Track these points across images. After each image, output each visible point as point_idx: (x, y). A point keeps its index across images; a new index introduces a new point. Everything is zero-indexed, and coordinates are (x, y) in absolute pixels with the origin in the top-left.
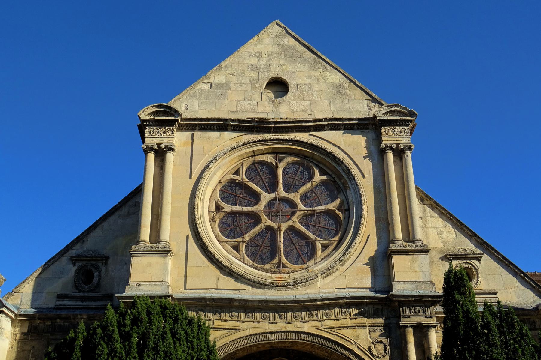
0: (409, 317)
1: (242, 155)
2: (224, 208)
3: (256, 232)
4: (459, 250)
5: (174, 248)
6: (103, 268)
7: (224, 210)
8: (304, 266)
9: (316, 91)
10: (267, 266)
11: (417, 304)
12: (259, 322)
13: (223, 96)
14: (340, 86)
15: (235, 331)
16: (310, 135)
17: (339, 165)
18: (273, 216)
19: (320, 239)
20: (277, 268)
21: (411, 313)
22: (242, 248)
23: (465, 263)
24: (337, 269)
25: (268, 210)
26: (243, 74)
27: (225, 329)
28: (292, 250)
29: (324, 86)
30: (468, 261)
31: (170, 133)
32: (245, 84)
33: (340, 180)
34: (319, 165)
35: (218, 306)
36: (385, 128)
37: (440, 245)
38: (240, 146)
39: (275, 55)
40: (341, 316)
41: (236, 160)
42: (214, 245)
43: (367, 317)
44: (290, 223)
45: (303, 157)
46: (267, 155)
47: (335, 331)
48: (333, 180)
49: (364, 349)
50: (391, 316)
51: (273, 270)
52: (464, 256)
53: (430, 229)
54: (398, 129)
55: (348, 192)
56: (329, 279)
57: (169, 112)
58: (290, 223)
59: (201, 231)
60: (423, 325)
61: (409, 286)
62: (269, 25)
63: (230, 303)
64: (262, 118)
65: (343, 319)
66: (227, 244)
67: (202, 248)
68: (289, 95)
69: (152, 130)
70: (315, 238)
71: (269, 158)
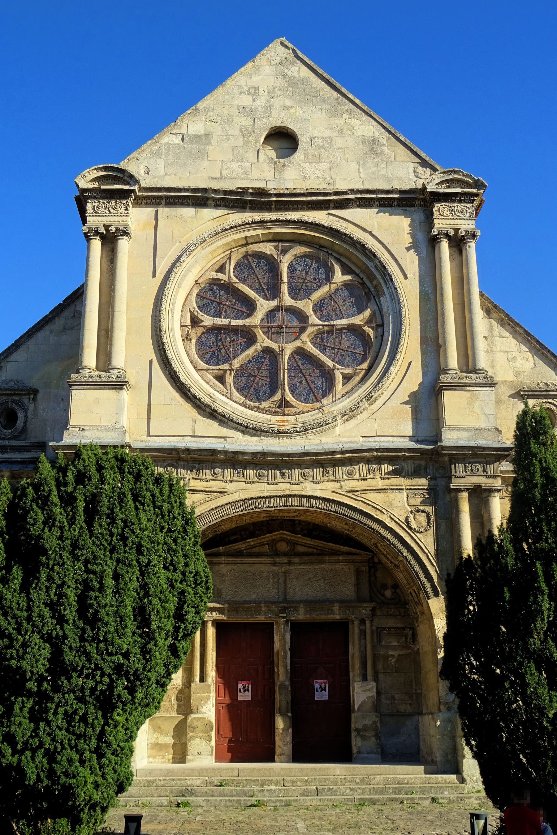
0: (463, 477)
1: (228, 244)
2: (202, 321)
3: (248, 356)
4: (538, 384)
5: (131, 377)
6: (31, 405)
7: (202, 324)
8: (318, 405)
9: (339, 148)
10: (265, 405)
11: (476, 460)
12: (253, 483)
13: (201, 154)
14: (374, 141)
15: (219, 494)
16: (329, 214)
17: (370, 259)
18: (274, 333)
19: (340, 367)
20: (279, 407)
21: (466, 471)
22: (229, 378)
23: (546, 402)
24: (364, 410)
25: (266, 324)
26: (230, 121)
28: (301, 382)
29: (350, 141)
30: (550, 401)
31: (123, 210)
32: (234, 137)
33: (371, 282)
34: (341, 259)
35: (195, 460)
36: (439, 205)
37: (510, 377)
38: (226, 230)
39: (279, 92)
40: (368, 475)
41: (221, 251)
42: (188, 374)
43: (404, 477)
44: (298, 343)
45: (318, 247)
46: (265, 244)
47: (360, 496)
48: (361, 281)
49: (400, 520)
50: (438, 475)
51: (273, 410)
52: (545, 393)
53: (498, 354)
54: (458, 206)
55: (382, 299)
56: (353, 422)
57: (122, 178)
58: (298, 343)
59: (170, 353)
60: (483, 488)
61: (465, 434)
62: (270, 45)
63: (212, 455)
64: (258, 189)
65: (371, 478)
66: (208, 373)
67: (172, 378)
68: (299, 155)
69: (96, 205)
70: (334, 365)
71: (269, 249)
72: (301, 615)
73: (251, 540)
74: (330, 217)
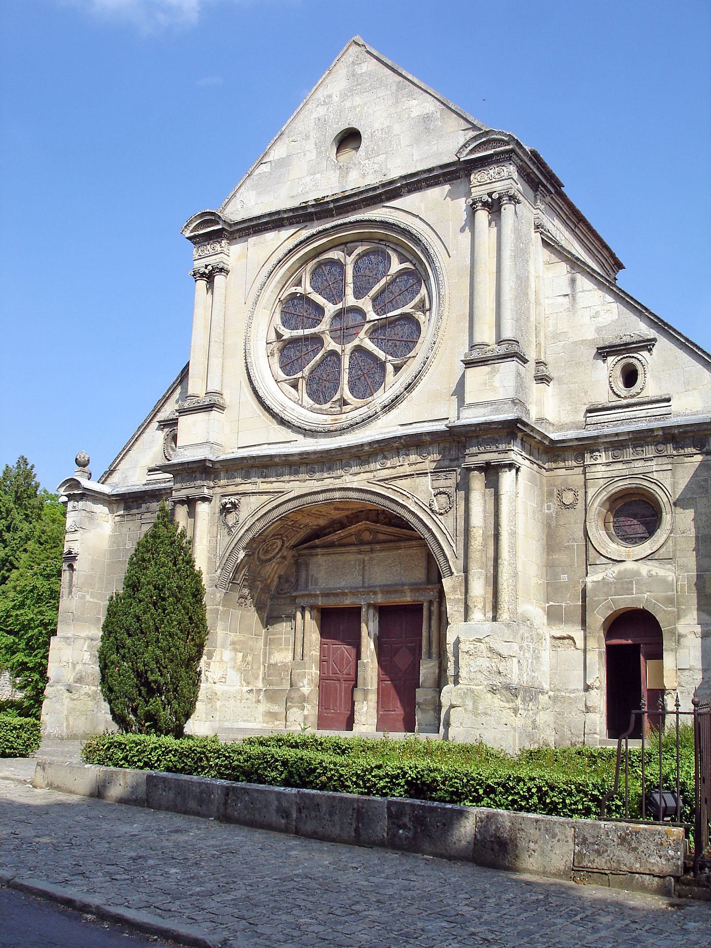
7: (283, 338)
8: (370, 399)
10: (329, 405)
14: (426, 119)
22: (302, 385)
23: (627, 357)
27: (269, 492)
30: (633, 355)
37: (590, 335)
41: (296, 267)
44: (356, 342)
56: (394, 412)
58: (356, 342)
65: (399, 466)
72: (380, 599)
73: (340, 531)
74: (384, 209)
